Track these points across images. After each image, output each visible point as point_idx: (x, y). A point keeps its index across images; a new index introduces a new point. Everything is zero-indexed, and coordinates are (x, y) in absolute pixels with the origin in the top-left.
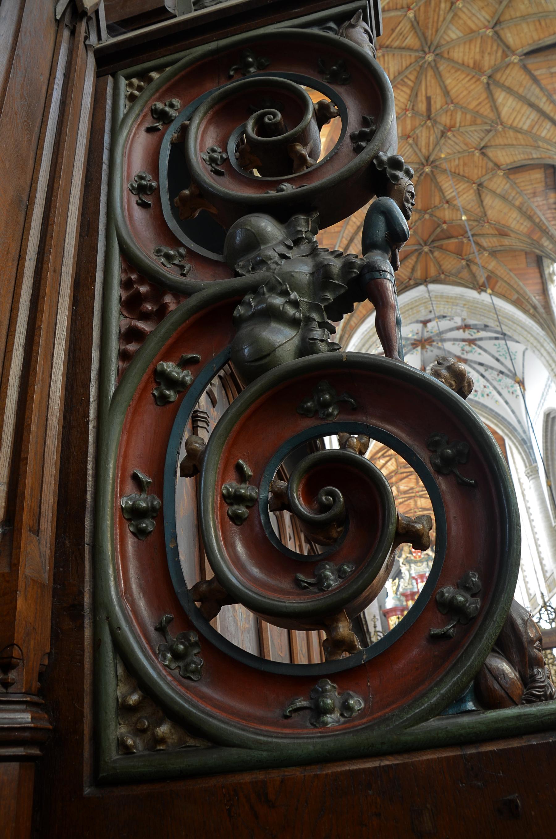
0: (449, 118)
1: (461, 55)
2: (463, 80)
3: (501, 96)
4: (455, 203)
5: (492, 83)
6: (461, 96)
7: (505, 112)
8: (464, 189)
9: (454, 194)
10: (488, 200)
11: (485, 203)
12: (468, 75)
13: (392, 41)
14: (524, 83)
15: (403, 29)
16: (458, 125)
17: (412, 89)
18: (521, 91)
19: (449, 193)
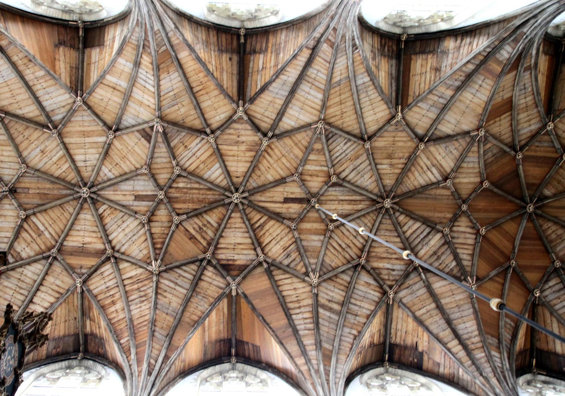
0: (315, 178)
1: (240, 164)
2: (269, 162)
3: (288, 122)
4: (448, 170)
5: (272, 133)
6: (288, 165)
7: (306, 118)
8: (428, 158)
9: (434, 170)
10: (446, 128)
11: (450, 132)
12: (264, 157)
13: (204, 238)
14: (270, 99)
15: (196, 226)
16: (325, 169)
17: (271, 218)
18: (281, 102)
19: (434, 176)
